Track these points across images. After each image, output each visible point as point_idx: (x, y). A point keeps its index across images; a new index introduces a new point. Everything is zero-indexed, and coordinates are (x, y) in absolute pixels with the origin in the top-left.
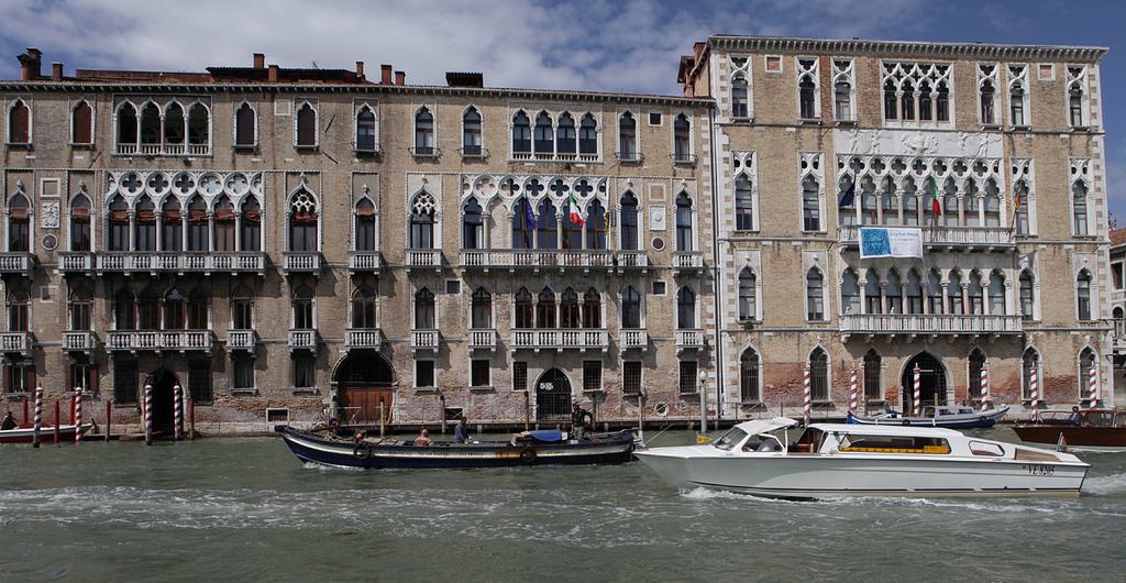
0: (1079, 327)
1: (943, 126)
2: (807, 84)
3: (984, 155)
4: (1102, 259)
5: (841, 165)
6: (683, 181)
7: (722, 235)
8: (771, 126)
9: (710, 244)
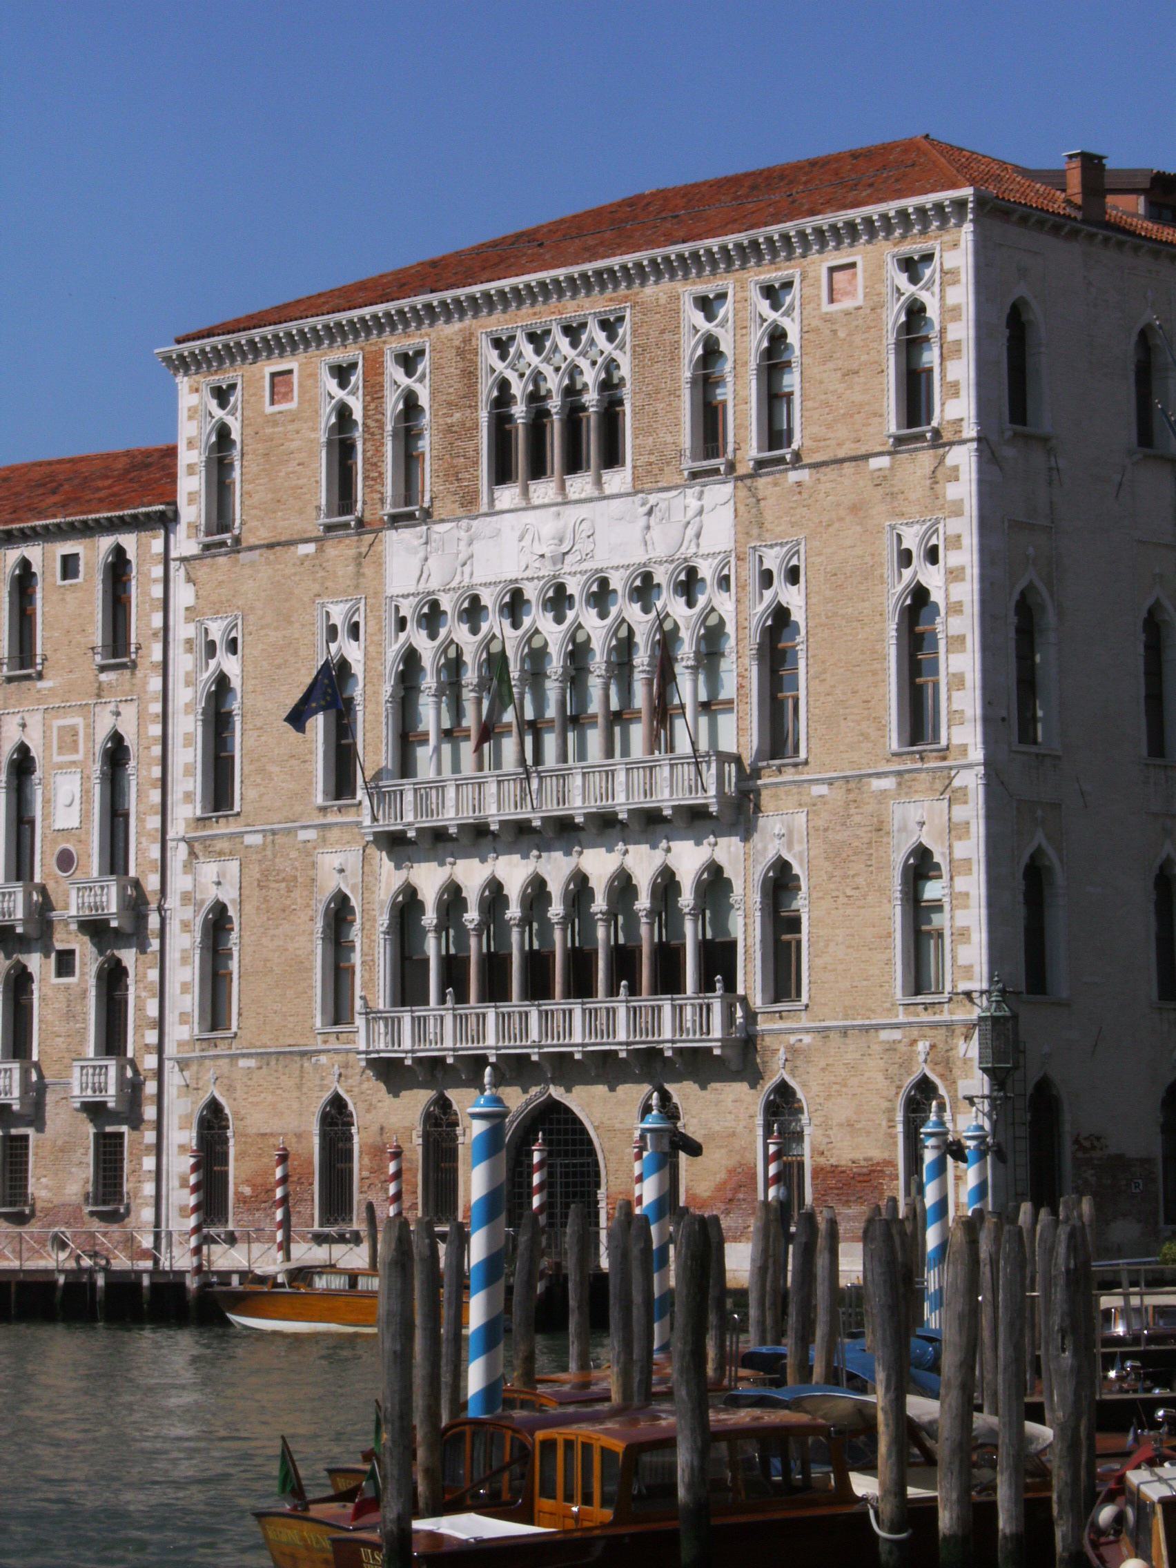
0: (902, 1018)
1: (617, 480)
2: (343, 412)
3: (693, 550)
4: (959, 813)
5: (402, 624)
7: (177, 829)
8: (270, 546)
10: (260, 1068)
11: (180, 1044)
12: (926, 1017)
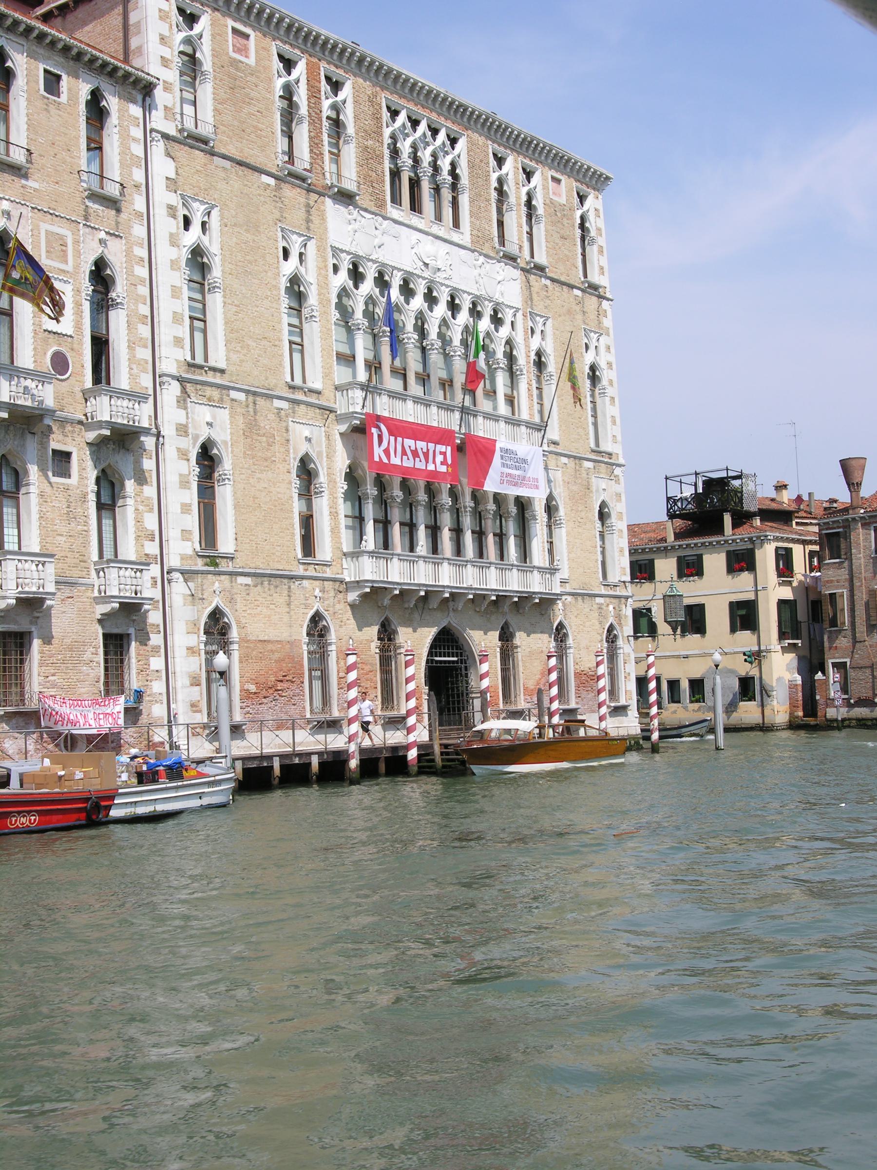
6: (102, 235)
8: (240, 163)
9: (146, 381)
10: (256, 586)
11: (183, 557)
12: (611, 593)
